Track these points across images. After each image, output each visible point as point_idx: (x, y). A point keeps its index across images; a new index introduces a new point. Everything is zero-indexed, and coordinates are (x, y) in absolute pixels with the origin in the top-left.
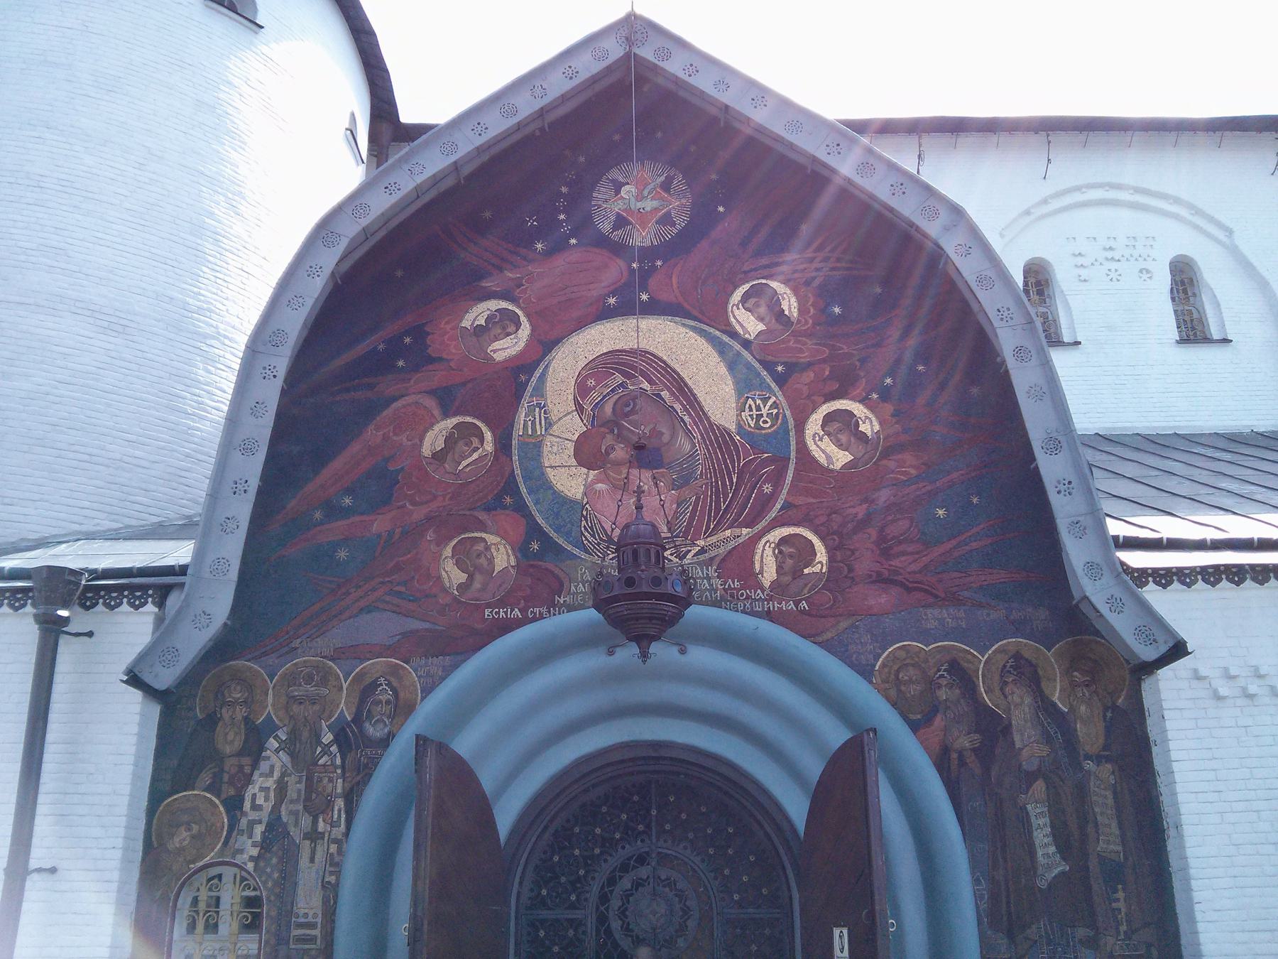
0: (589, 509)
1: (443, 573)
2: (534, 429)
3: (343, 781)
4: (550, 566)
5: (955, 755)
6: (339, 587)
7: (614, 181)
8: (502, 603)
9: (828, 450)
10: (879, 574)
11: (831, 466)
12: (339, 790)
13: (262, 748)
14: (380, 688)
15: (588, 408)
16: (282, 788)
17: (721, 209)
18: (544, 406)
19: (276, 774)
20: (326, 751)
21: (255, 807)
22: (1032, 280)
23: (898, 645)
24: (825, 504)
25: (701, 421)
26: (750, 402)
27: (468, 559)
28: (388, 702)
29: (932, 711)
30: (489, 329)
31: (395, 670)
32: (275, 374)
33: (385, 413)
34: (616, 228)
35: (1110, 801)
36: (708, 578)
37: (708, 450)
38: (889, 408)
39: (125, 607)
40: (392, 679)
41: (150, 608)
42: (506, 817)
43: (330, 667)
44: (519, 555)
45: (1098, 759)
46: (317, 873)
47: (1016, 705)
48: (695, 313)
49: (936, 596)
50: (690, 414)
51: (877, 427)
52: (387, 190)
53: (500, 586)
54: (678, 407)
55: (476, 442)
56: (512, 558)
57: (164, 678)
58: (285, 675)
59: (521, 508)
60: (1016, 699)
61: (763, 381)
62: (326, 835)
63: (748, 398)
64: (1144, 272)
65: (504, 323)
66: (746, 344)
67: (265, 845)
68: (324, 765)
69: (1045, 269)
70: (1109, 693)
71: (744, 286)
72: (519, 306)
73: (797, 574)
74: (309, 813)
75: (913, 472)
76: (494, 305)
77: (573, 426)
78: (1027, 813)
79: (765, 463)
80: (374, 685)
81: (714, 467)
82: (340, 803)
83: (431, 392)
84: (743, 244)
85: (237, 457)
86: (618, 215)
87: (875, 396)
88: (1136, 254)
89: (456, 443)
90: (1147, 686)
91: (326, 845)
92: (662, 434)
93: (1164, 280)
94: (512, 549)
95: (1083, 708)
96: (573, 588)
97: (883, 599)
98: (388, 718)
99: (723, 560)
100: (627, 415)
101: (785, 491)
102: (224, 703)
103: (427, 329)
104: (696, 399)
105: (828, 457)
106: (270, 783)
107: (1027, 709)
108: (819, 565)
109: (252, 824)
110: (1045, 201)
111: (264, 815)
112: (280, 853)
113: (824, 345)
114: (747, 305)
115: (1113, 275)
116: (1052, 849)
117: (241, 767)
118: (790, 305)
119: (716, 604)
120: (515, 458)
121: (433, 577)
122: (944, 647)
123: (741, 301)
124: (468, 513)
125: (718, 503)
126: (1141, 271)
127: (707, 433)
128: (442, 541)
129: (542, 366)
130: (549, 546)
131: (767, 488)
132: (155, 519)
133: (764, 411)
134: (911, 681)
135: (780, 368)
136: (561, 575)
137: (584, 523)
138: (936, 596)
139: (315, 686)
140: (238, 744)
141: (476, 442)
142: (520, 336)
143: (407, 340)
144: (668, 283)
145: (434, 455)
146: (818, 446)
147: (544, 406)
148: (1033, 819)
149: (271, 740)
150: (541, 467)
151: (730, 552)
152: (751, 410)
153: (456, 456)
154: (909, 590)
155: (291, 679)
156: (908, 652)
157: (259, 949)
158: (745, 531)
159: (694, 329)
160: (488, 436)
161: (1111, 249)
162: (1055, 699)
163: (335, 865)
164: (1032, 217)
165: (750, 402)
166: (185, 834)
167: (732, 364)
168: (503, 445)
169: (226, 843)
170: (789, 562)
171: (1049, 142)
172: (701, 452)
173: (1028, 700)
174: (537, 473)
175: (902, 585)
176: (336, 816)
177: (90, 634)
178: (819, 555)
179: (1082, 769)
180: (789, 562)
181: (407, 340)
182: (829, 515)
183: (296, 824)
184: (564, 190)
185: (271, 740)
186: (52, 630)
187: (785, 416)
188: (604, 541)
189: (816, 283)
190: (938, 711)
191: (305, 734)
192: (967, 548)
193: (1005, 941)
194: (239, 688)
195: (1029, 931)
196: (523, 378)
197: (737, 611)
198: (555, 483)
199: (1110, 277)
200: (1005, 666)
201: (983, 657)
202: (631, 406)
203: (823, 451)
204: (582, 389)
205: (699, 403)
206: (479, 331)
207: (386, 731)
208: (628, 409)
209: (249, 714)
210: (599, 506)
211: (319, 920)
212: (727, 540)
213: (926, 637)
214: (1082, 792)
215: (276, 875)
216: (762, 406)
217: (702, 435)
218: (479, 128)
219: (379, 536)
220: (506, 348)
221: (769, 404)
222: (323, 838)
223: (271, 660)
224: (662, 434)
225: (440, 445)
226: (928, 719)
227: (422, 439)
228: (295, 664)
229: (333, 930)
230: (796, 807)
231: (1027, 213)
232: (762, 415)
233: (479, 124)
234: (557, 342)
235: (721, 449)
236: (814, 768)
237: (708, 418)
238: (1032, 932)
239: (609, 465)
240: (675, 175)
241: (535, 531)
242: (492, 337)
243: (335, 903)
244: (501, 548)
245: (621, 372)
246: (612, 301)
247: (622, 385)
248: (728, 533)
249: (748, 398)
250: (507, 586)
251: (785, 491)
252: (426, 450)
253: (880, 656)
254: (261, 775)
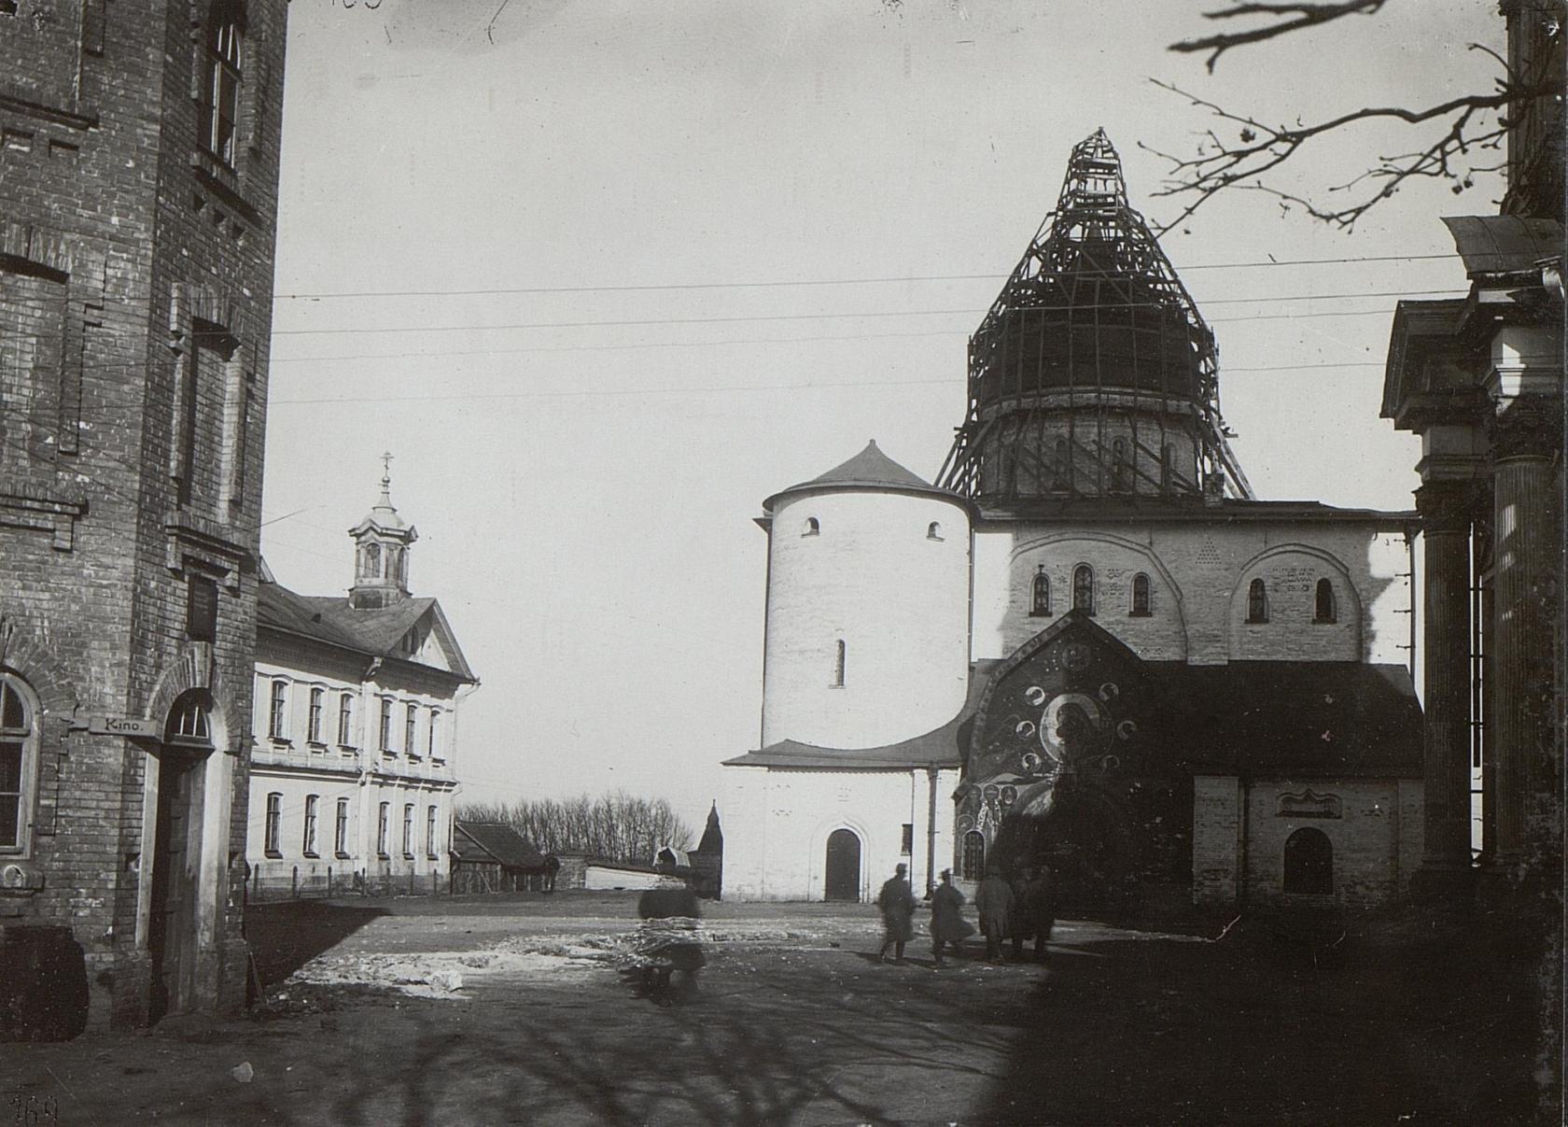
16: (987, 815)
65: (1037, 694)
76: (1035, 688)
118: (1116, 691)
168: (1037, 729)
186: (933, 779)
204: (1058, 714)
220: (1038, 701)
234: (1052, 700)
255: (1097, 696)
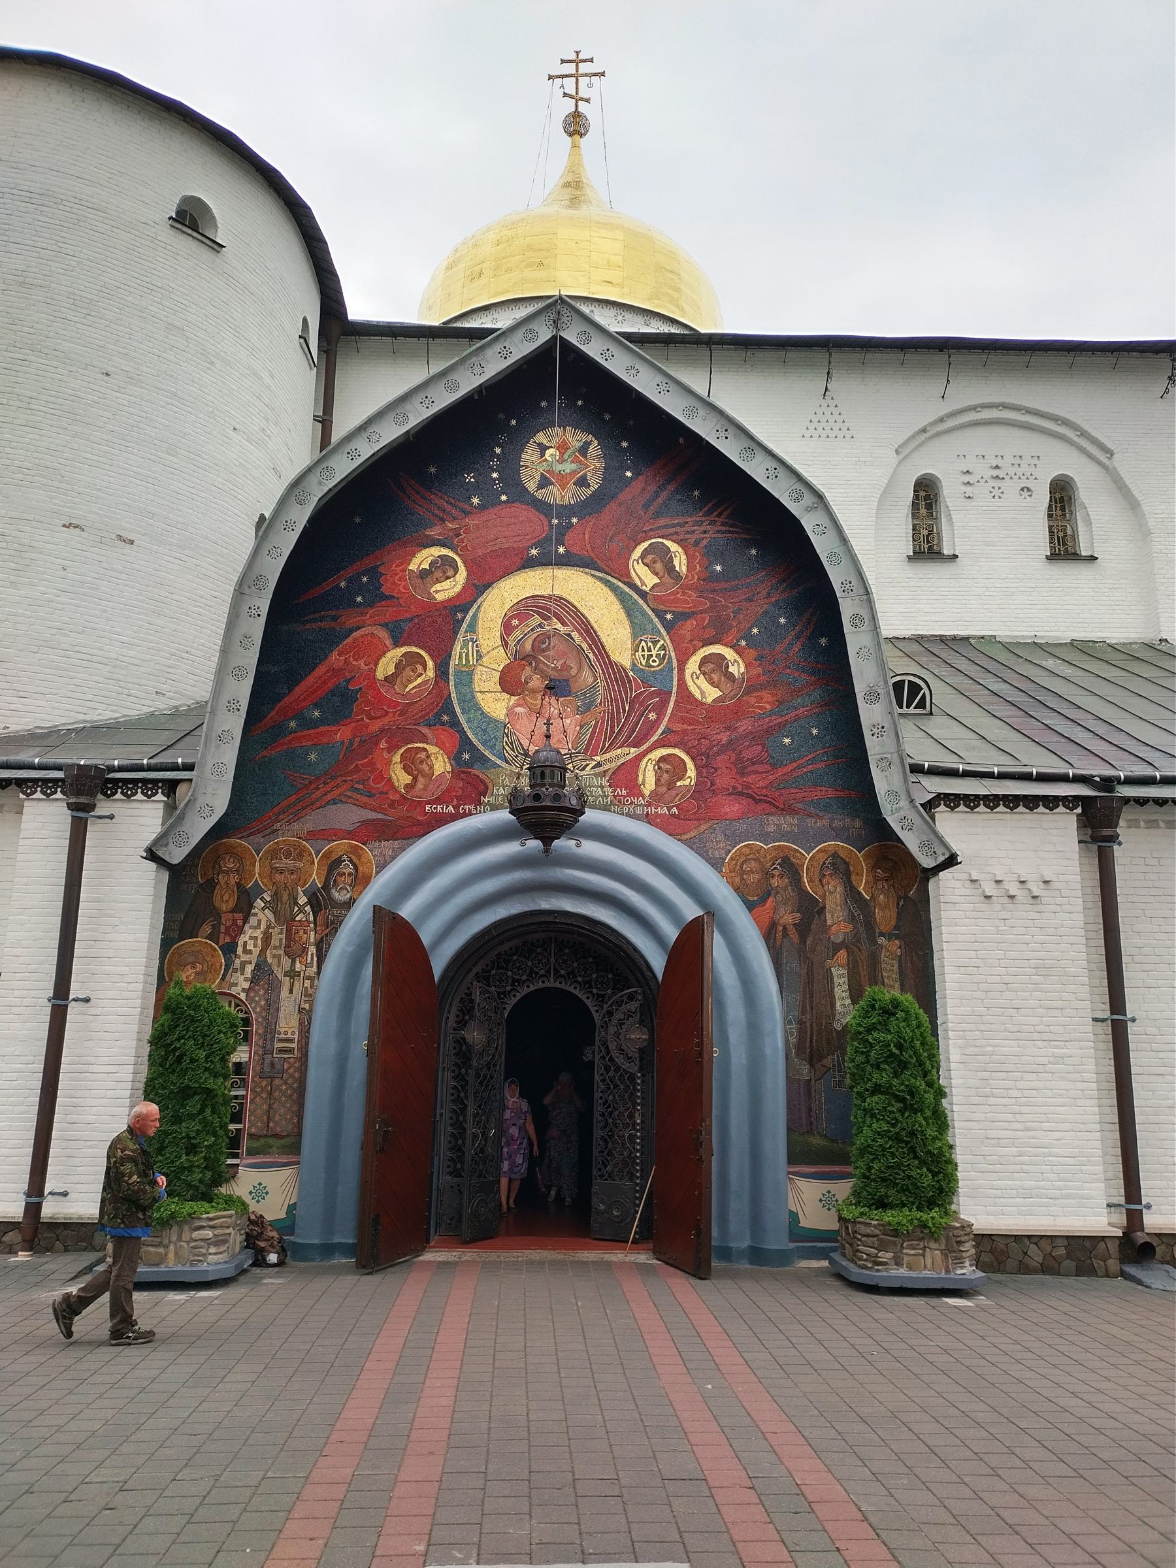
0: (510, 727)
1: (393, 775)
2: (467, 660)
3: (316, 933)
4: (477, 772)
5: (781, 928)
6: (311, 783)
7: (540, 445)
8: (438, 801)
9: (703, 686)
10: (733, 787)
11: (704, 700)
12: (312, 940)
13: (251, 907)
14: (344, 863)
15: (512, 643)
16: (267, 938)
17: (629, 474)
18: (476, 641)
19: (263, 927)
20: (301, 911)
21: (246, 951)
22: (923, 494)
23: (744, 844)
24: (697, 730)
25: (603, 657)
26: (643, 643)
27: (412, 764)
28: (350, 874)
29: (767, 894)
30: (432, 572)
31: (355, 850)
32: (259, 613)
33: (345, 642)
34: (541, 486)
35: (896, 968)
36: (602, 787)
37: (607, 682)
38: (752, 653)
39: (139, 796)
40: (353, 857)
41: (160, 797)
42: (439, 964)
43: (304, 846)
44: (453, 763)
45: (890, 937)
46: (295, 1001)
47: (831, 893)
48: (601, 564)
49: (777, 807)
50: (594, 652)
51: (743, 669)
52: (349, 455)
53: (438, 787)
54: (585, 646)
55: (420, 668)
56: (448, 764)
57: (176, 854)
58: (267, 852)
59: (455, 724)
60: (831, 888)
61: (655, 628)
62: (302, 973)
63: (641, 640)
64: (1025, 490)
65: (443, 568)
66: (643, 595)
67: (254, 980)
68: (300, 921)
69: (935, 483)
70: (902, 887)
71: (643, 544)
72: (457, 554)
73: (671, 786)
74: (289, 957)
75: (768, 707)
77: (496, 659)
78: (832, 974)
79: (652, 695)
80: (339, 861)
81: (611, 698)
82: (312, 950)
83: (385, 625)
84: (646, 506)
85: (230, 682)
86: (542, 474)
87: (743, 643)
88: (1020, 474)
89: (404, 669)
90: (932, 884)
91: (302, 981)
92: (572, 668)
93: (1043, 497)
94: (449, 758)
95: (882, 897)
96: (495, 791)
97: (736, 807)
98: (350, 886)
99: (614, 773)
100: (544, 651)
101: (666, 719)
102: (220, 871)
103: (381, 570)
104: (599, 640)
105: (702, 693)
106: (258, 933)
107: (838, 896)
108: (689, 780)
109: (243, 964)
110: (941, 420)
111: (254, 958)
112: (266, 986)
113: (706, 598)
114: (645, 561)
115: (996, 492)
116: (848, 1001)
117: (235, 921)
118: (680, 562)
119: (606, 808)
120: (452, 683)
121: (385, 778)
122: (779, 846)
123: (640, 557)
124: (413, 727)
125: (613, 727)
126: (1022, 489)
127: (607, 669)
128: (392, 749)
129: (475, 606)
130: (478, 758)
131: (652, 716)
132: (148, 710)
133: (654, 652)
134: (752, 872)
135: (669, 616)
136: (487, 781)
137: (505, 739)
138: (777, 807)
139: (292, 860)
140: (231, 904)
141: (420, 668)
142: (457, 580)
143: (365, 579)
144: (582, 534)
145: (386, 678)
146: (695, 683)
147: (476, 641)
148: (835, 979)
149: (258, 900)
150: (472, 692)
151: (620, 766)
152: (643, 651)
153: (404, 679)
154: (757, 801)
155: (274, 854)
156: (751, 849)
157: (250, 1058)
158: (632, 750)
159: (601, 579)
160: (430, 664)
161: (997, 467)
162: (861, 889)
163: (309, 996)
164: (928, 435)
165: (643, 643)
166: (191, 971)
167: (630, 610)
168: (442, 671)
169: (223, 979)
170: (666, 776)
171: (950, 364)
172: (601, 685)
173: (840, 889)
174: (469, 696)
175: (752, 797)
176: (309, 960)
177: (111, 817)
178: (689, 771)
179: (876, 942)
180: (666, 776)
181: (365, 579)
182: (701, 739)
183: (279, 966)
184: (498, 450)
185: (258, 900)
187: (670, 657)
188: (520, 754)
189: (705, 542)
190: (770, 895)
191: (285, 897)
192: (805, 770)
193: (808, 1066)
194: (232, 860)
195: (825, 1061)
196: (459, 616)
197: (623, 814)
198: (483, 705)
199: (993, 494)
200: (824, 863)
201: (808, 855)
202: (547, 644)
203: (699, 688)
204: (507, 628)
205: (601, 644)
206: (424, 574)
207: (348, 896)
208: (544, 646)
209: (241, 879)
210: (518, 726)
211: (296, 1037)
212: (618, 756)
213: (765, 837)
214: (874, 960)
215: (263, 1003)
216: (652, 648)
217: (603, 670)
218: (427, 402)
219: (342, 743)
220: (446, 590)
221: (658, 646)
222: (299, 976)
223: (258, 838)
224: (572, 668)
225: (391, 670)
226: (763, 900)
227: (376, 664)
228: (277, 843)
229: (307, 1044)
230: (657, 962)
231: (924, 430)
232: (652, 656)
233: (427, 397)
234: (488, 586)
235: (617, 682)
236: (672, 933)
237: (608, 657)
238: (828, 1061)
239: (527, 692)
240: (592, 441)
241: (466, 743)
242: (435, 579)
243: (309, 1024)
244: (440, 758)
245: (539, 613)
246: (534, 552)
247: (540, 625)
248: (619, 751)
249: (641, 640)
250: (444, 787)
251: (666, 719)
252: (380, 674)
253: (730, 852)
254: (251, 927)
255: (624, 575)
